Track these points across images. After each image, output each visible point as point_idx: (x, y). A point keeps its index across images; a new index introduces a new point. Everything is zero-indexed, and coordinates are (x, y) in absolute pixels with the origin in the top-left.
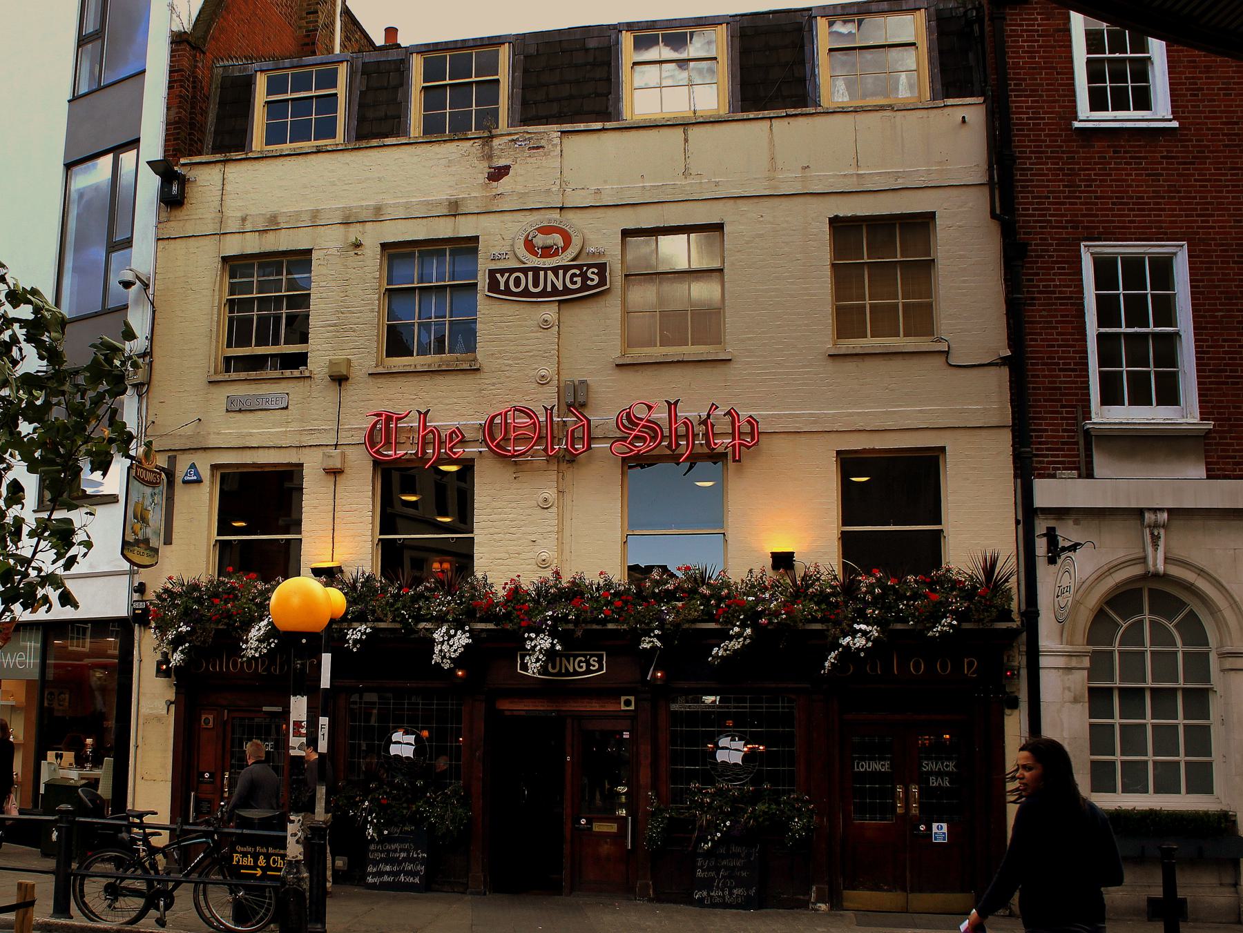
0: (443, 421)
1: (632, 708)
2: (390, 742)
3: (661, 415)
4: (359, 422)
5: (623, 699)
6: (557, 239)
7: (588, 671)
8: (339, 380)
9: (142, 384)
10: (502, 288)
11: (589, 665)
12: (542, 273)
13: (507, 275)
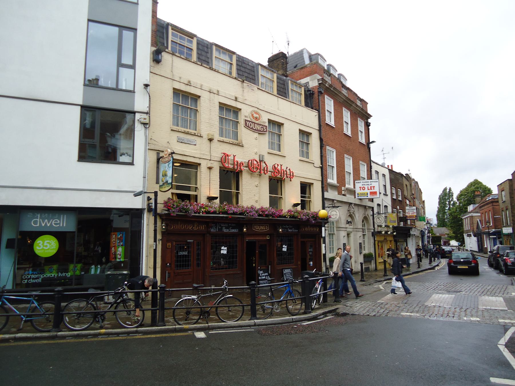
0: (239, 159)
2: (221, 250)
3: (279, 168)
4: (217, 155)
5: (268, 236)
6: (257, 116)
8: (211, 140)
9: (147, 124)
10: (248, 125)
11: (266, 228)
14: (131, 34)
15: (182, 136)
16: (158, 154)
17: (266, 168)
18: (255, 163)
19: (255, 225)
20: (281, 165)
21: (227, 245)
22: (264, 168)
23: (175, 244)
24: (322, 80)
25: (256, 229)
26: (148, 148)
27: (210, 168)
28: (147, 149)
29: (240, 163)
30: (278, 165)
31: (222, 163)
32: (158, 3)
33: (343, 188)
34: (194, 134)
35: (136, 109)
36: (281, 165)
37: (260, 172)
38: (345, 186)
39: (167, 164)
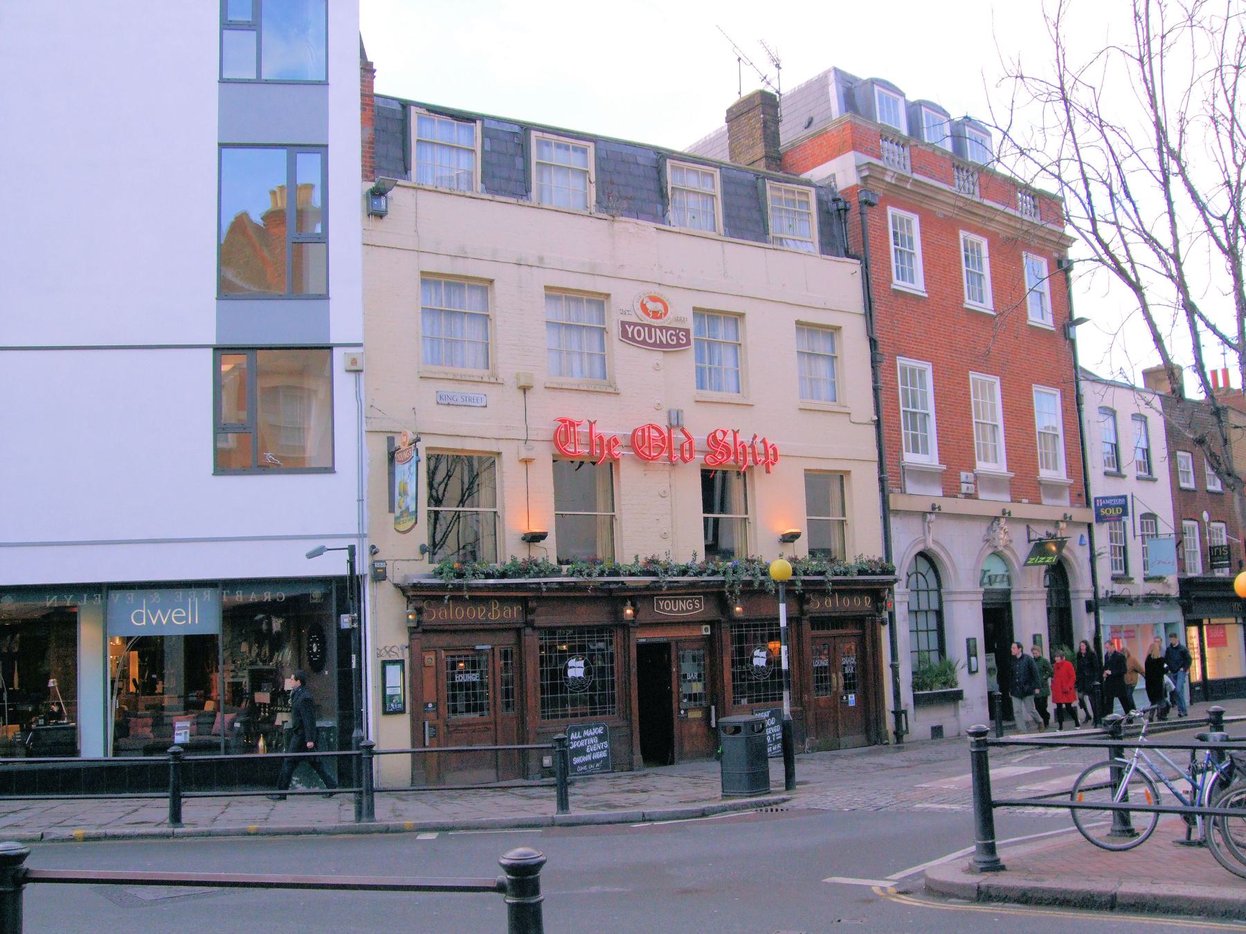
0: (605, 429)
1: (709, 633)
2: (567, 667)
3: (729, 439)
4: (543, 425)
5: (704, 627)
6: (659, 307)
7: (694, 609)
8: (525, 389)
10: (630, 336)
11: (694, 605)
12: (653, 329)
13: (632, 327)
14: (317, 158)
15: (448, 388)
16: (391, 440)
17: (687, 446)
18: (654, 433)
19: (662, 600)
20: (735, 433)
21: (585, 655)
22: (682, 446)
23: (447, 657)
24: (869, 169)
25: (664, 610)
26: (365, 428)
27: (526, 461)
28: (364, 432)
29: (609, 441)
30: (725, 433)
31: (557, 445)
32: (375, 71)
33: (963, 475)
34: (480, 379)
35: (333, 341)
36: (735, 433)
37: (670, 457)
38: (971, 467)
39: (407, 465)
